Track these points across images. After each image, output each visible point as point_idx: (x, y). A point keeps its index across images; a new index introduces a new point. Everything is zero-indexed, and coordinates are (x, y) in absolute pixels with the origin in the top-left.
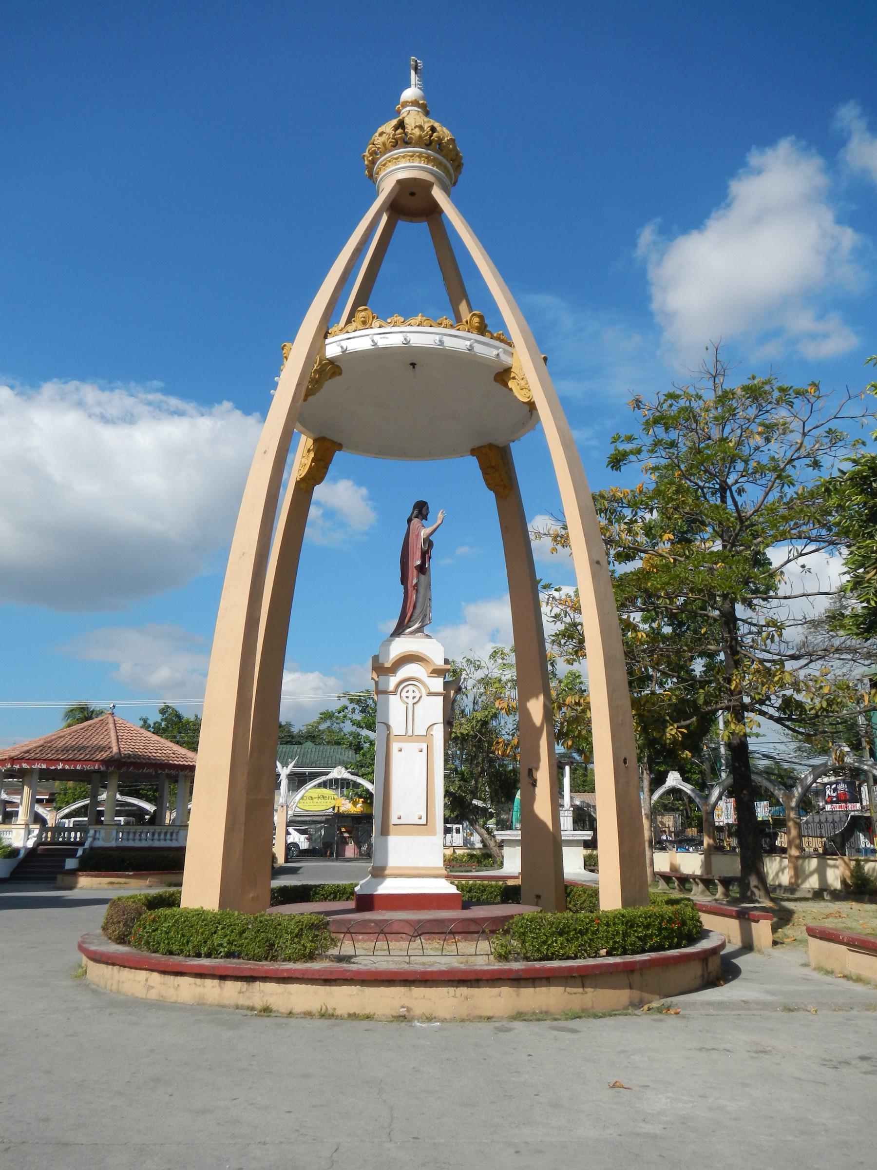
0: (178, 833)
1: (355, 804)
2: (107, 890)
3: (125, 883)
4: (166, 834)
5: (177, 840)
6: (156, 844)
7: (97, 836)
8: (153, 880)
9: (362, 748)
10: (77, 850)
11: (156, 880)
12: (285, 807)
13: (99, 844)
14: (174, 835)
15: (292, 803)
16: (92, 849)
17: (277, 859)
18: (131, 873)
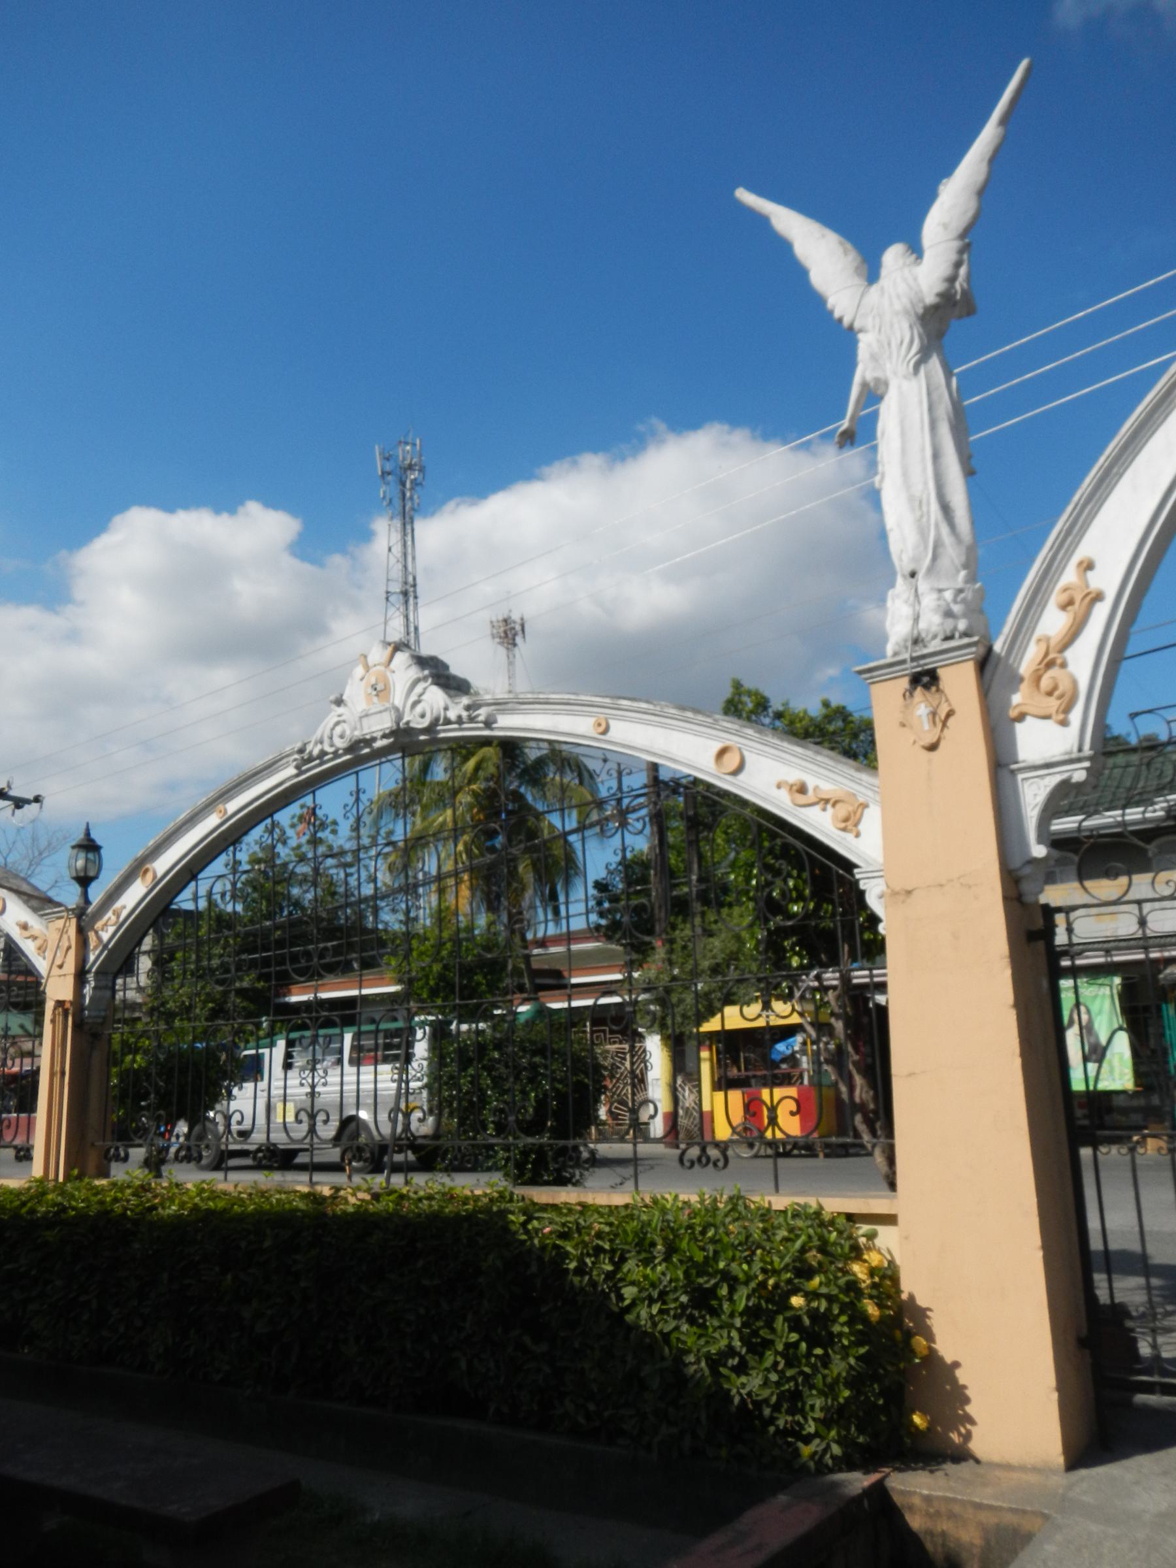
15: (1053, 622)
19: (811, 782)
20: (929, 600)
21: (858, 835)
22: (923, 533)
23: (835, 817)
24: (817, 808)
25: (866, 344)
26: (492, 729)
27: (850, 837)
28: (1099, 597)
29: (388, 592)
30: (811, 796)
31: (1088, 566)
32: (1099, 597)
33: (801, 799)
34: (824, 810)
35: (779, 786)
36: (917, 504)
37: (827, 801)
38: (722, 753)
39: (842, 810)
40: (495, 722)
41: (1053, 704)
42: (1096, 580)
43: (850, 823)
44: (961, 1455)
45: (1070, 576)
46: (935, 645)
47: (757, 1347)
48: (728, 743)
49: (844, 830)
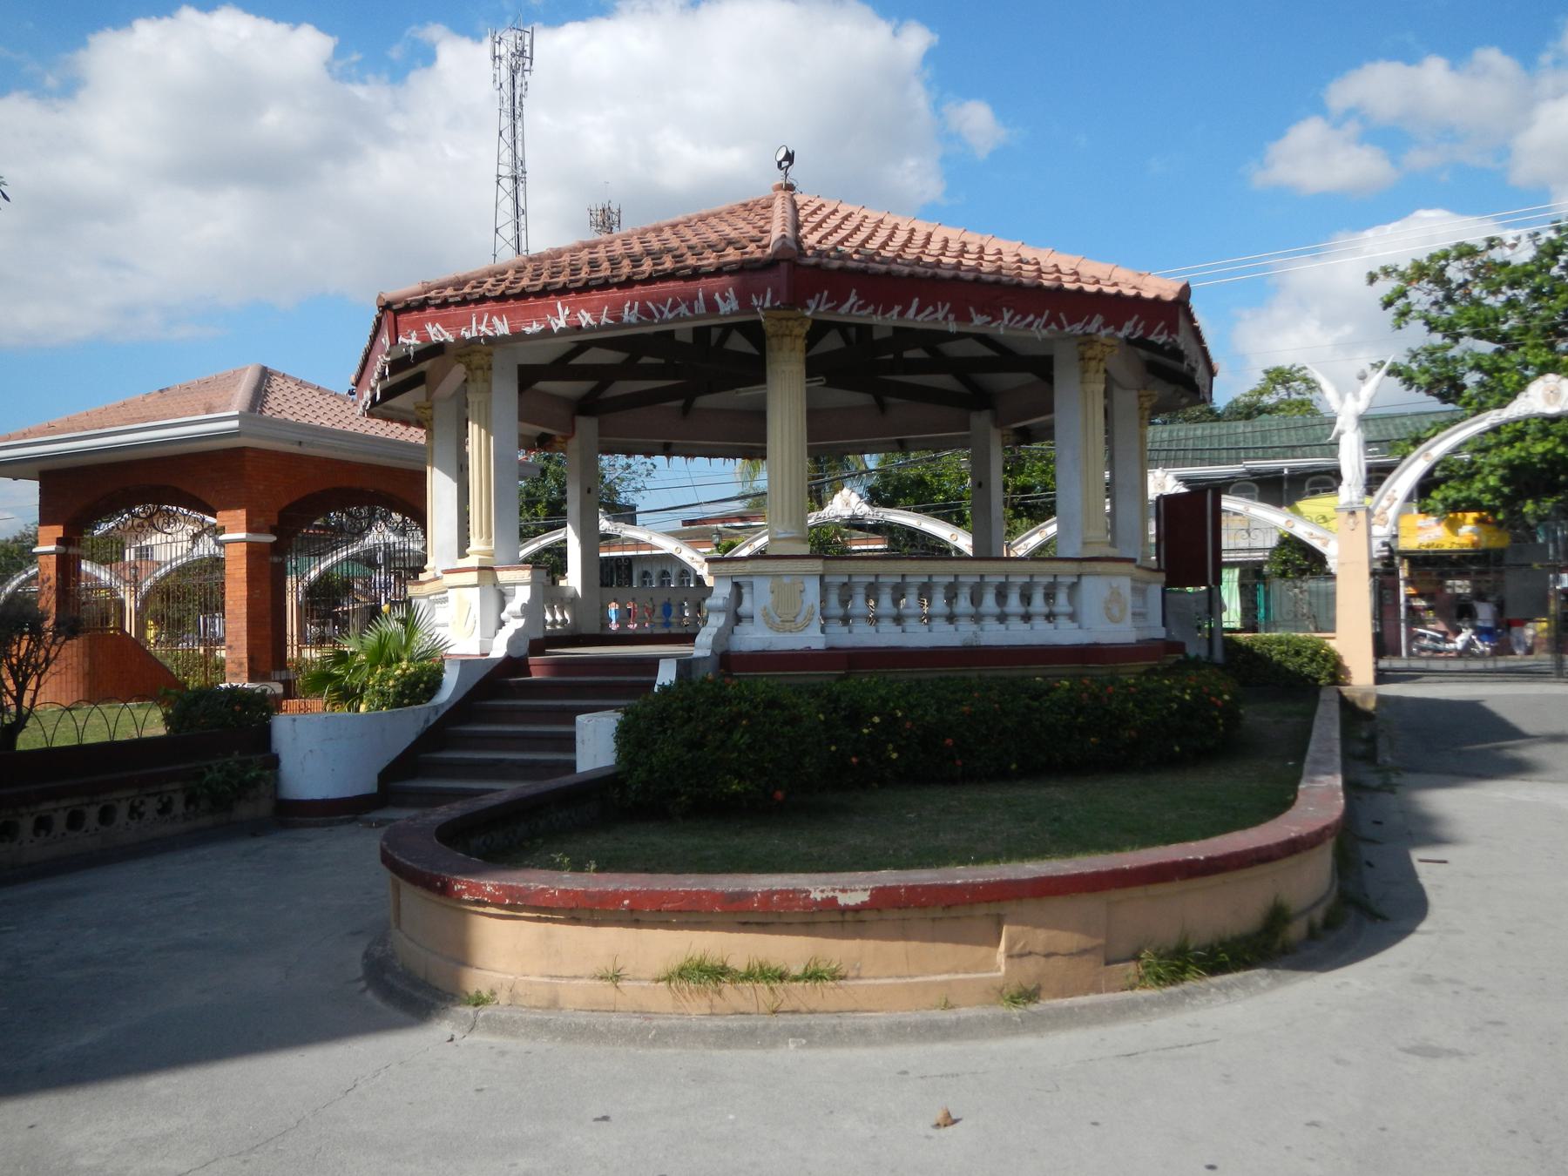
0: (1073, 588)
1: (1454, 526)
2: (664, 1037)
3: (813, 976)
4: (1001, 595)
5: (1072, 617)
6: (994, 634)
7: (746, 607)
8: (1040, 938)
9: (1464, 387)
10: (651, 665)
11: (1069, 940)
12: (1361, 515)
13: (754, 637)
14: (1062, 597)
15: (1384, 503)
16: (727, 660)
17: (1346, 672)
18: (854, 890)
20: (1354, 493)
22: (1353, 474)
25: (1340, 420)
28: (1396, 499)
29: (498, 176)
31: (1394, 491)
32: (1396, 499)
36: (1353, 467)
41: (1383, 523)
42: (1396, 495)
43: (1325, 544)
44: (1349, 685)
45: (1389, 492)
46: (1356, 505)
47: (1312, 660)
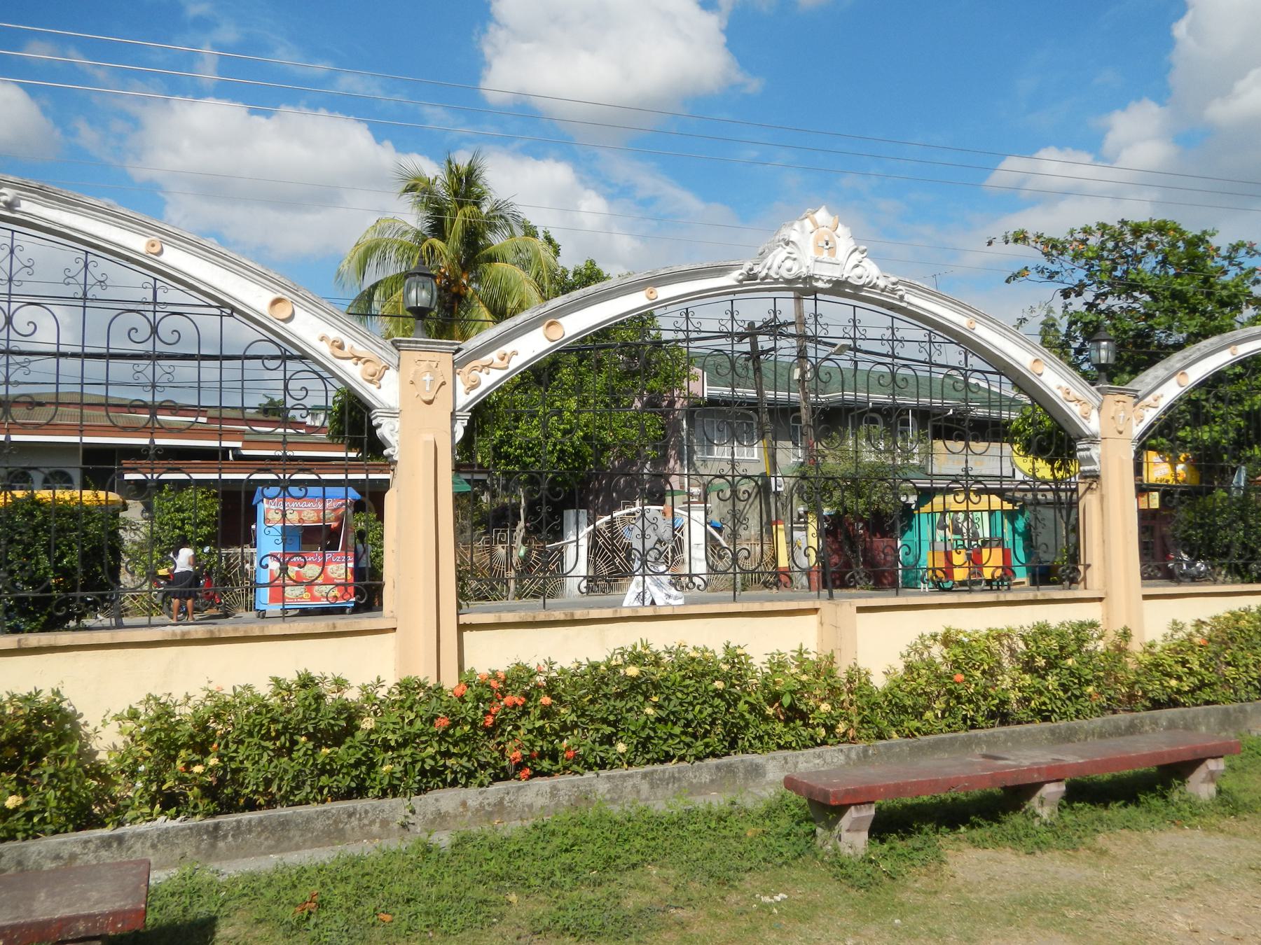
19: (348, 343)
21: (379, 388)
23: (364, 371)
24: (351, 362)
26: (14, 212)
27: (372, 388)
30: (346, 352)
33: (339, 353)
34: (356, 364)
35: (322, 339)
37: (359, 359)
38: (276, 302)
39: (371, 368)
40: (19, 206)
43: (375, 378)
48: (284, 297)
49: (371, 382)
